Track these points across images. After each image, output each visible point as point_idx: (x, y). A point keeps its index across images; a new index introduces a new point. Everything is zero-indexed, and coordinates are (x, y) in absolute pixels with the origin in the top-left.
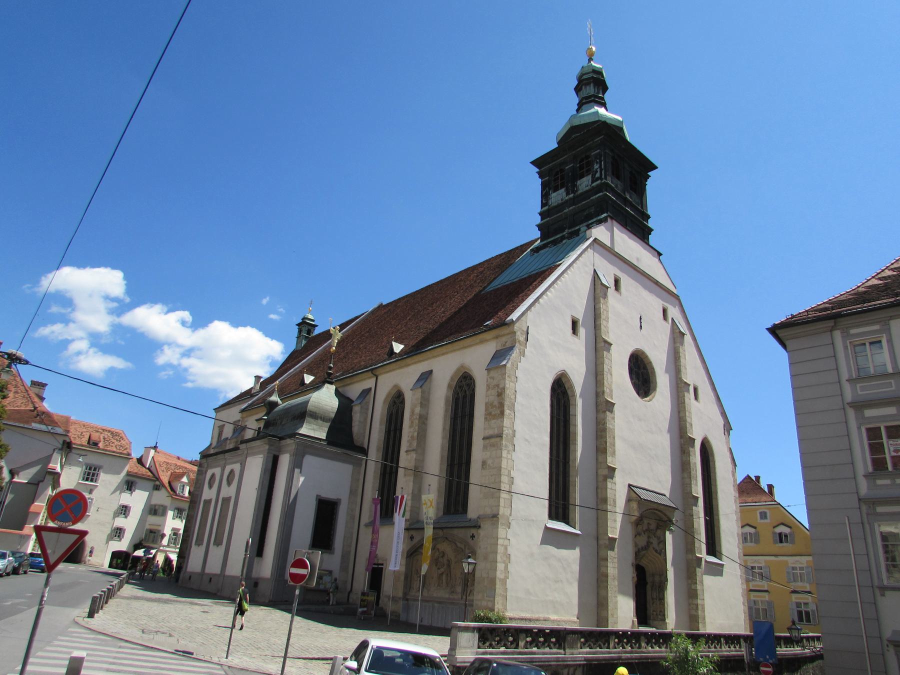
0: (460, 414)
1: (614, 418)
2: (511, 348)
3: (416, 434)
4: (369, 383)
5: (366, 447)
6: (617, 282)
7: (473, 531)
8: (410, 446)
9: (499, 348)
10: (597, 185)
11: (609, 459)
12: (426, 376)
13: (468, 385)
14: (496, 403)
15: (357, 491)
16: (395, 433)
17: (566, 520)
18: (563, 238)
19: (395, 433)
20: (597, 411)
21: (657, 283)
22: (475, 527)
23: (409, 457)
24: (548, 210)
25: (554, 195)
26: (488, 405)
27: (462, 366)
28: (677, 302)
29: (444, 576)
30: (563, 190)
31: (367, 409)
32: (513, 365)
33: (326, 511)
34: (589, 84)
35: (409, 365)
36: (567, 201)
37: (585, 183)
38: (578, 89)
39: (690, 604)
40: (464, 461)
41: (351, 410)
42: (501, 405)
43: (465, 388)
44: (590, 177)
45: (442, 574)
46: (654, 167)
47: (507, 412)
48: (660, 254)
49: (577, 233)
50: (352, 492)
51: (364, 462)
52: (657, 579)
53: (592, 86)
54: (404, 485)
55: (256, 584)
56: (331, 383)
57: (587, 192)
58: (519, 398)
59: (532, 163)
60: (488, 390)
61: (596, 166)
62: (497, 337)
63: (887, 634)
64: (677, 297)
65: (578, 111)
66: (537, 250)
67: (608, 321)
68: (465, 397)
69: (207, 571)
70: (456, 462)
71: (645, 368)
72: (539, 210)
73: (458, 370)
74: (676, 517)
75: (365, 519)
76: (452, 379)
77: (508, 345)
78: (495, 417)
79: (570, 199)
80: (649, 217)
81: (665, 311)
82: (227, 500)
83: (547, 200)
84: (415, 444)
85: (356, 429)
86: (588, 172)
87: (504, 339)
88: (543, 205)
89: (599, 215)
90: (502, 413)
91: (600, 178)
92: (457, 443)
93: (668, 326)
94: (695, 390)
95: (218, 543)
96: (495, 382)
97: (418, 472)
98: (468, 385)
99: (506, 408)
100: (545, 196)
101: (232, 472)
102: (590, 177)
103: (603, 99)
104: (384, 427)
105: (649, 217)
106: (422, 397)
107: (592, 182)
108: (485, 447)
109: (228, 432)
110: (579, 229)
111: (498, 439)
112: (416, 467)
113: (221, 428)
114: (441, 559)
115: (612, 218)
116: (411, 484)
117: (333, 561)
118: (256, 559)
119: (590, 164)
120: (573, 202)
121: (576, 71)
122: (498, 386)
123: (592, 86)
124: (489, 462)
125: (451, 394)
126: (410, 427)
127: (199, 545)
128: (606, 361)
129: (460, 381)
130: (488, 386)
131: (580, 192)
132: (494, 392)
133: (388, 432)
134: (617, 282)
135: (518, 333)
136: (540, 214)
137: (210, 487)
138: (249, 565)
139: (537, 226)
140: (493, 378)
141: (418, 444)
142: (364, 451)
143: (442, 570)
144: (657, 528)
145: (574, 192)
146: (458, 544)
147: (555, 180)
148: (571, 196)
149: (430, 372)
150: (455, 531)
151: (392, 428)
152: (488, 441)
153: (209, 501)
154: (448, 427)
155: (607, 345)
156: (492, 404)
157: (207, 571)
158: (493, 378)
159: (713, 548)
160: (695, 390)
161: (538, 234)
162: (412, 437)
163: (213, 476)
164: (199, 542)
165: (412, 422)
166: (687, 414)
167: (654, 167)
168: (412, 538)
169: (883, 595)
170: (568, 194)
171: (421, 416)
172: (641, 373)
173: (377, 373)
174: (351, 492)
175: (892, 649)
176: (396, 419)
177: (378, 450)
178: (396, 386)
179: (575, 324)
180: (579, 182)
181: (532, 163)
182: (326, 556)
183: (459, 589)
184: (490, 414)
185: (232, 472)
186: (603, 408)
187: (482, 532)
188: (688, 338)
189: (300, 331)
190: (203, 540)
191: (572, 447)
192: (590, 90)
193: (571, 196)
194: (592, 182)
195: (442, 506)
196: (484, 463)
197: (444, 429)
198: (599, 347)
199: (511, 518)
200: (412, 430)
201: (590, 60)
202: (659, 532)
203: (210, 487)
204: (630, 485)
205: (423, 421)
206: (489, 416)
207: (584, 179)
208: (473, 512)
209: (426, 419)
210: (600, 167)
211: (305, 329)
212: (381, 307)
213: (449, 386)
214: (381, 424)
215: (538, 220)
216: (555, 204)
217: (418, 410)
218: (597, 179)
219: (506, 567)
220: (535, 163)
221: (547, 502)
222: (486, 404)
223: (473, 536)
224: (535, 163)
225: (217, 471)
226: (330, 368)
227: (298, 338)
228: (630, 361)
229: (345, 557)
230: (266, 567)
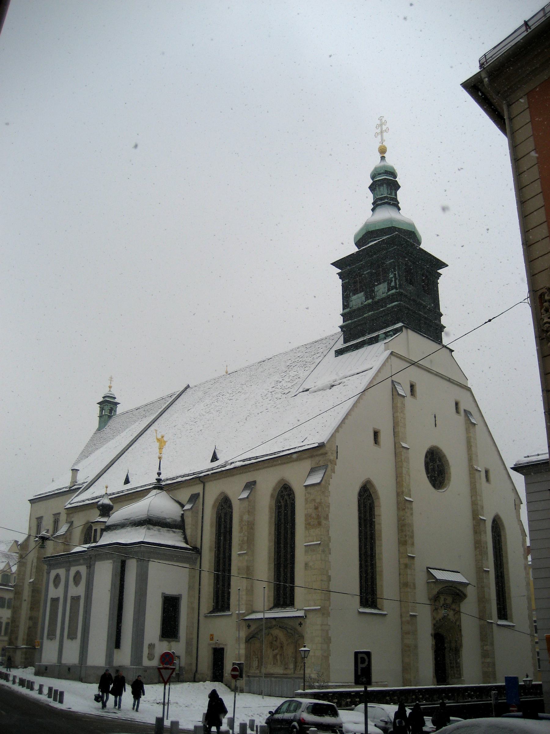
1: (412, 514)
3: (246, 538)
6: (412, 387)
7: (300, 620)
10: (393, 295)
11: (409, 549)
13: (289, 495)
14: (314, 515)
17: (374, 605)
20: (398, 509)
21: (449, 380)
23: (241, 558)
24: (349, 313)
25: (354, 297)
26: (308, 516)
28: (469, 393)
29: (278, 657)
31: (197, 513)
33: (171, 605)
34: (382, 185)
35: (234, 475)
37: (381, 290)
38: (372, 188)
39: (483, 663)
44: (386, 285)
45: (276, 655)
46: (443, 265)
47: (324, 522)
48: (452, 351)
50: (191, 588)
51: (199, 559)
52: (453, 645)
57: (382, 299)
58: (332, 508)
59: (333, 264)
60: (306, 504)
61: (391, 276)
62: (312, 457)
64: (469, 389)
65: (373, 210)
67: (405, 428)
68: (286, 505)
69: (64, 661)
71: (440, 460)
72: (341, 312)
73: (279, 482)
74: (471, 592)
75: (204, 610)
76: (274, 490)
77: (321, 463)
79: (369, 305)
80: (441, 315)
81: (457, 404)
82: (76, 599)
83: (347, 302)
84: (245, 547)
87: (317, 459)
88: (345, 307)
89: (395, 324)
90: (319, 524)
93: (461, 418)
94: (487, 472)
95: (72, 636)
97: (248, 573)
98: (289, 495)
101: (78, 574)
102: (386, 283)
103: (396, 200)
104: (214, 529)
105: (441, 315)
107: (389, 290)
109: (47, 523)
113: (39, 520)
114: (274, 643)
115: (407, 328)
117: (178, 648)
118: (116, 651)
119: (386, 272)
120: (370, 307)
121: (370, 169)
122: (314, 500)
124: (311, 564)
127: (51, 640)
128: (405, 464)
130: (306, 500)
131: (377, 298)
134: (412, 387)
135: (329, 454)
136: (342, 315)
137: (56, 585)
138: (110, 657)
139: (341, 327)
143: (276, 651)
144: (453, 602)
145: (373, 298)
146: (289, 631)
147: (355, 282)
148: (370, 301)
153: (55, 601)
154: (273, 532)
155: (405, 450)
157: (64, 661)
159: (503, 613)
160: (487, 472)
163: (57, 576)
164: (51, 635)
165: (242, 528)
166: (478, 498)
167: (443, 265)
168: (249, 626)
170: (367, 298)
172: (436, 467)
178: (222, 493)
179: (376, 434)
180: (376, 289)
181: (333, 264)
182: (173, 644)
183: (291, 666)
185: (78, 574)
186: (403, 506)
187: (308, 621)
188: (480, 427)
189: (102, 409)
191: (377, 542)
192: (384, 191)
193: (370, 301)
194: (389, 290)
195: (272, 599)
196: (306, 564)
197: (270, 533)
198: (399, 452)
199: (330, 608)
201: (383, 158)
202: (453, 606)
203: (56, 585)
204: (427, 568)
205: (251, 526)
206: (308, 526)
207: (381, 286)
209: (253, 524)
211: (107, 408)
213: (272, 496)
214: (211, 527)
215: (340, 321)
216: (355, 307)
217: (246, 517)
219: (328, 647)
220: (336, 264)
222: (306, 515)
223: (300, 624)
224: (336, 264)
225: (62, 572)
227: (100, 417)
228: (426, 457)
229: (188, 643)
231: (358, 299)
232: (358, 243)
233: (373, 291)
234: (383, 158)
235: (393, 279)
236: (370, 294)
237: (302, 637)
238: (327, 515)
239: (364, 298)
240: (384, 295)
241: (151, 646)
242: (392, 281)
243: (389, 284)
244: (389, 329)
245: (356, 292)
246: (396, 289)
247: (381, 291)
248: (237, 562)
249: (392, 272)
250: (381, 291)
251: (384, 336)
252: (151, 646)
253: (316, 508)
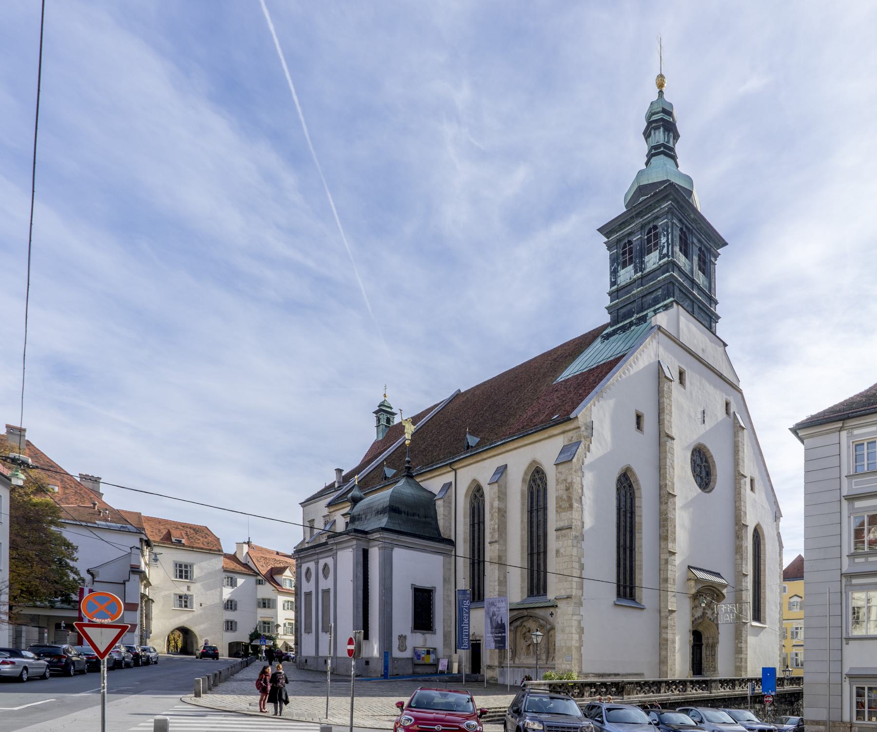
0: (535, 507)
2: (578, 443)
3: (496, 526)
5: (453, 539)
7: (552, 610)
8: (492, 537)
9: (566, 443)
14: (565, 497)
15: (450, 577)
16: (479, 525)
19: (479, 525)
22: (553, 606)
24: (618, 291)
25: (622, 272)
26: (559, 499)
32: (578, 460)
36: (635, 281)
37: (652, 260)
40: (542, 550)
42: (570, 498)
43: (539, 482)
47: (575, 505)
50: (446, 580)
51: (453, 553)
54: (491, 573)
55: (367, 663)
57: (654, 271)
63: (846, 670)
70: (535, 551)
73: (531, 464)
78: (564, 510)
84: (496, 536)
88: (613, 284)
90: (571, 506)
92: (535, 534)
96: (563, 477)
97: (501, 563)
99: (574, 501)
100: (614, 273)
104: (468, 520)
106: (499, 491)
107: (660, 259)
108: (558, 537)
111: (568, 531)
112: (500, 557)
116: (497, 572)
118: (364, 643)
124: (562, 551)
125: (526, 488)
126: (491, 520)
129: (533, 475)
131: (647, 270)
132: (563, 487)
133: (473, 525)
140: (561, 473)
141: (500, 535)
142: (452, 543)
145: (642, 270)
148: (639, 274)
150: (537, 611)
151: (476, 521)
152: (559, 532)
154: (526, 520)
156: (561, 498)
157: (320, 654)
158: (561, 473)
161: (607, 319)
162: (494, 529)
169: (847, 644)
170: (636, 272)
171: (499, 509)
174: (444, 580)
175: (847, 679)
176: (479, 512)
177: (465, 542)
180: (647, 258)
187: (559, 611)
190: (311, 628)
193: (639, 274)
194: (660, 259)
195: (526, 590)
196: (557, 551)
200: (493, 522)
205: (502, 513)
206: (559, 509)
208: (551, 594)
209: (505, 512)
213: (524, 480)
216: (623, 284)
218: (664, 257)
221: (615, 585)
222: (557, 498)
230: (374, 649)
231: (627, 274)
233: (642, 262)
236: (640, 267)
237: (553, 628)
238: (581, 498)
240: (655, 266)
241: (402, 638)
243: (660, 253)
245: (624, 266)
247: (651, 262)
248: (490, 552)
250: (651, 262)
252: (402, 638)
253: (567, 489)
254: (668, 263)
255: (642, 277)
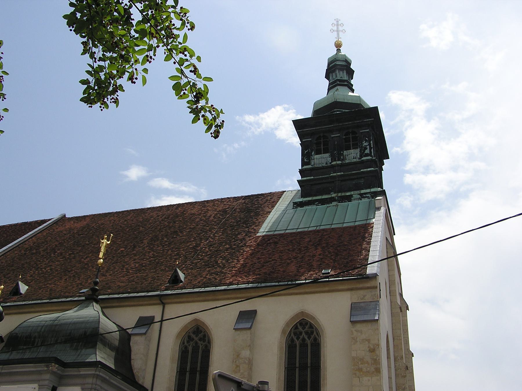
4: (153, 311)
12: (248, 317)
13: (309, 335)
18: (332, 200)
25: (317, 156)
27: (302, 313)
30: (327, 155)
41: (129, 340)
49: (349, 199)
53: (339, 71)
56: (97, 301)
57: (355, 163)
62: (351, 290)
66: (297, 205)
68: (303, 345)
73: (297, 315)
76: (287, 324)
85: (137, 363)
86: (355, 147)
87: (362, 292)
91: (370, 154)
98: (309, 335)
104: (175, 366)
107: (361, 156)
110: (351, 196)
123: (339, 71)
129: (296, 327)
130: (354, 340)
131: (347, 161)
133: (181, 372)
136: (301, 172)
149: (255, 312)
156: (362, 360)
165: (237, 366)
173: (164, 301)
180: (345, 153)
184: (360, 370)
201: (339, 50)
210: (370, 145)
212: (63, 219)
213: (283, 332)
218: (367, 155)
226: (96, 283)
232: (315, 112)
234: (339, 50)
235: (368, 147)
239: (329, 159)
240: (355, 160)
242: (367, 148)
244: (363, 191)
245: (318, 152)
246: (372, 156)
249: (366, 141)
251: (359, 196)
254: (371, 160)
255: (341, 165)
